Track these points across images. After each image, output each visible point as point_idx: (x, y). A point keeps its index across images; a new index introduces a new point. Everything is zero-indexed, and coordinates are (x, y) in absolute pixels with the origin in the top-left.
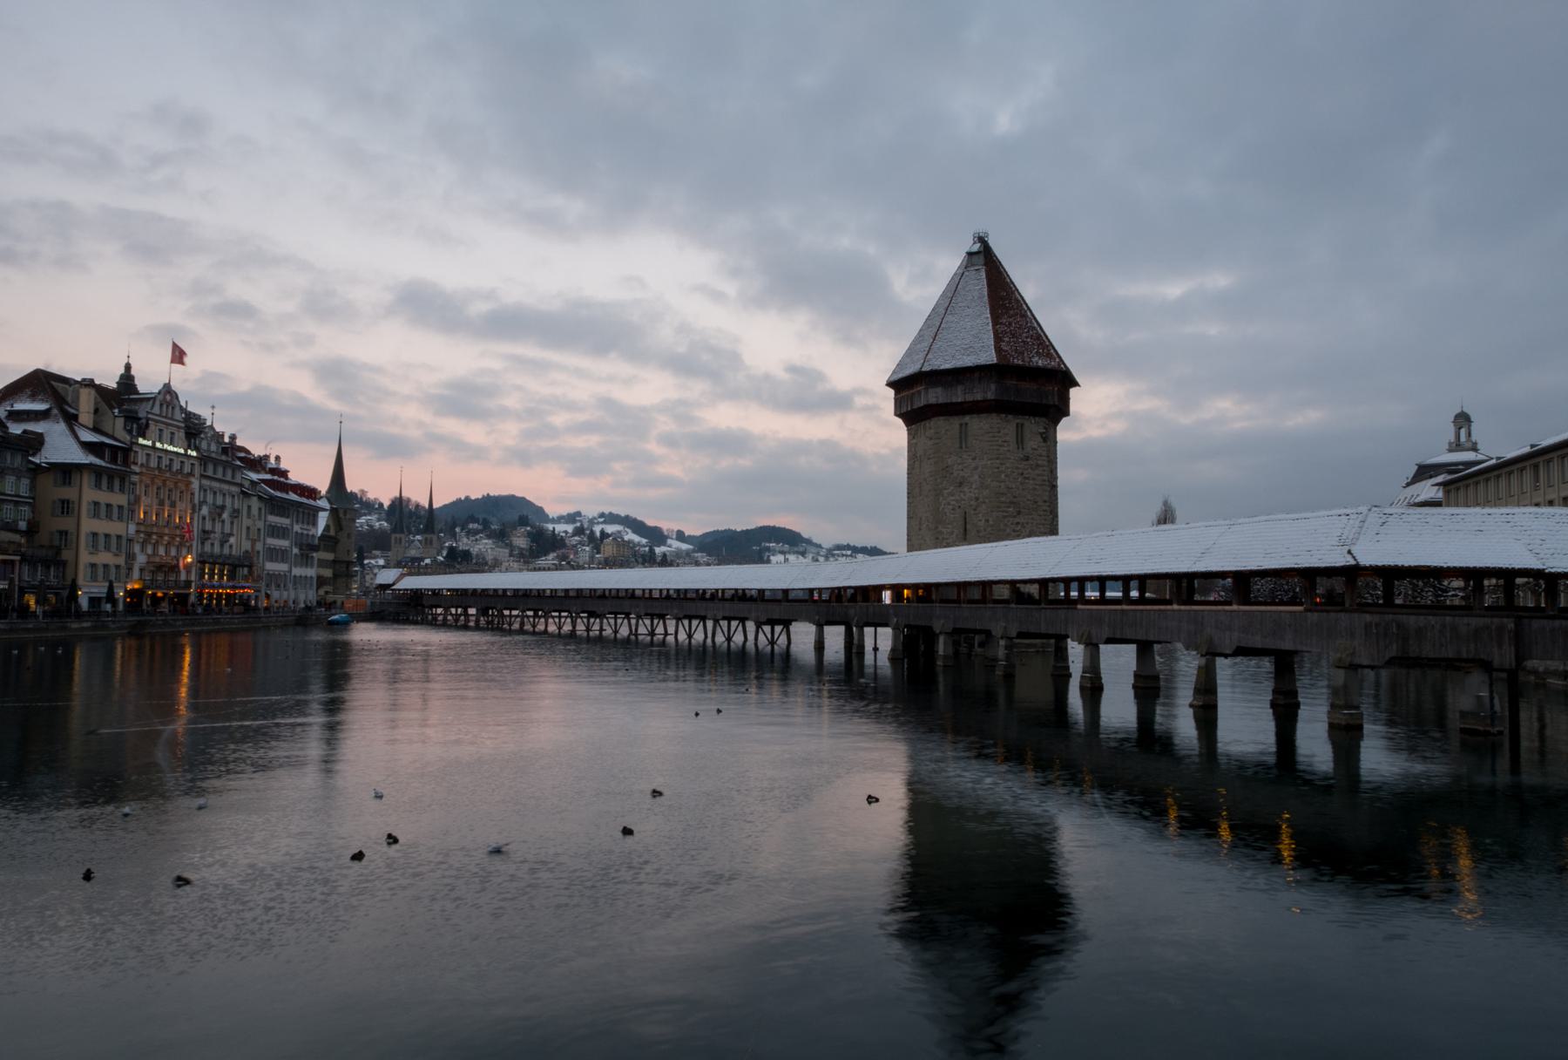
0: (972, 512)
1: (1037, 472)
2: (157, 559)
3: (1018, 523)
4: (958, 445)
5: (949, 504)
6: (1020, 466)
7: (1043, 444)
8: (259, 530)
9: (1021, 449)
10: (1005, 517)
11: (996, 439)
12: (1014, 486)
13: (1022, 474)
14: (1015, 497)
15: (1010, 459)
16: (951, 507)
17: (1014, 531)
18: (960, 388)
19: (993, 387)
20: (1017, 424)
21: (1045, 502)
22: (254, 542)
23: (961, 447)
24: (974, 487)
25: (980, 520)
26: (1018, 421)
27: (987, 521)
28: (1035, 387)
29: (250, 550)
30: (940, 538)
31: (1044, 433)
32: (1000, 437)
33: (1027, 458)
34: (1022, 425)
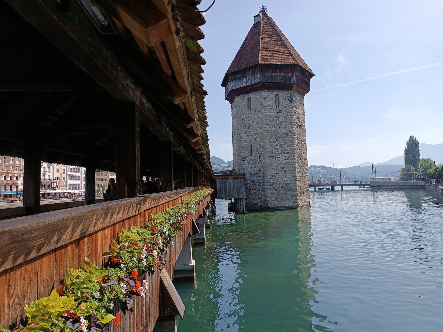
0: (254, 141)
2: (5, 182)
3: (277, 145)
4: (246, 108)
5: (244, 138)
6: (278, 116)
7: (291, 104)
8: (64, 170)
9: (278, 107)
11: (264, 103)
14: (275, 132)
15: (272, 113)
16: (244, 140)
17: (275, 149)
19: (259, 76)
22: (61, 174)
24: (254, 128)
25: (258, 145)
27: (261, 145)
28: (283, 75)
29: (59, 177)
30: (240, 156)
31: (290, 98)
33: (281, 112)
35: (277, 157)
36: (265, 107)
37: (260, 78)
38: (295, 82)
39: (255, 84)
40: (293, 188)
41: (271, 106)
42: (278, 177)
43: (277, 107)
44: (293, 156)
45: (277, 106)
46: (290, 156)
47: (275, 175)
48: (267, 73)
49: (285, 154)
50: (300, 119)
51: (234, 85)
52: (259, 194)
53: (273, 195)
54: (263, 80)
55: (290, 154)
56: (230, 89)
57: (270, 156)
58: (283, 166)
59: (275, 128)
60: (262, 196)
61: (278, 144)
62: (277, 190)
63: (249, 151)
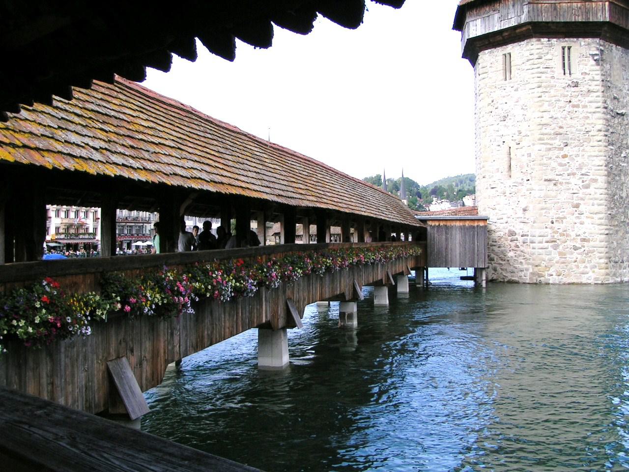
1: (590, 99)
3: (565, 156)
6: (566, 93)
7: (598, 68)
10: (550, 149)
12: (559, 115)
13: (570, 102)
14: (561, 127)
17: (560, 165)
18: (496, 16)
19: (526, 9)
20: (563, 48)
21: (600, 131)
23: (506, 80)
26: (564, 44)
30: (487, 177)
31: (596, 55)
32: (541, 63)
33: (576, 85)
34: (569, 48)
35: (564, 181)
36: (539, 75)
37: (529, 12)
38: (608, 20)
39: (520, 26)
40: (595, 249)
41: (553, 71)
42: (564, 224)
43: (566, 75)
44: (599, 181)
45: (567, 71)
46: (594, 179)
47: (560, 220)
48: (544, 2)
49: (581, 177)
50: (621, 100)
51: (477, 27)
52: (523, 261)
53: (552, 264)
54: (536, 17)
55: (594, 177)
56: (467, 37)
57: (550, 180)
58: (577, 202)
59: (562, 119)
60: (528, 264)
61: (566, 153)
62: (560, 254)
63: (506, 166)
